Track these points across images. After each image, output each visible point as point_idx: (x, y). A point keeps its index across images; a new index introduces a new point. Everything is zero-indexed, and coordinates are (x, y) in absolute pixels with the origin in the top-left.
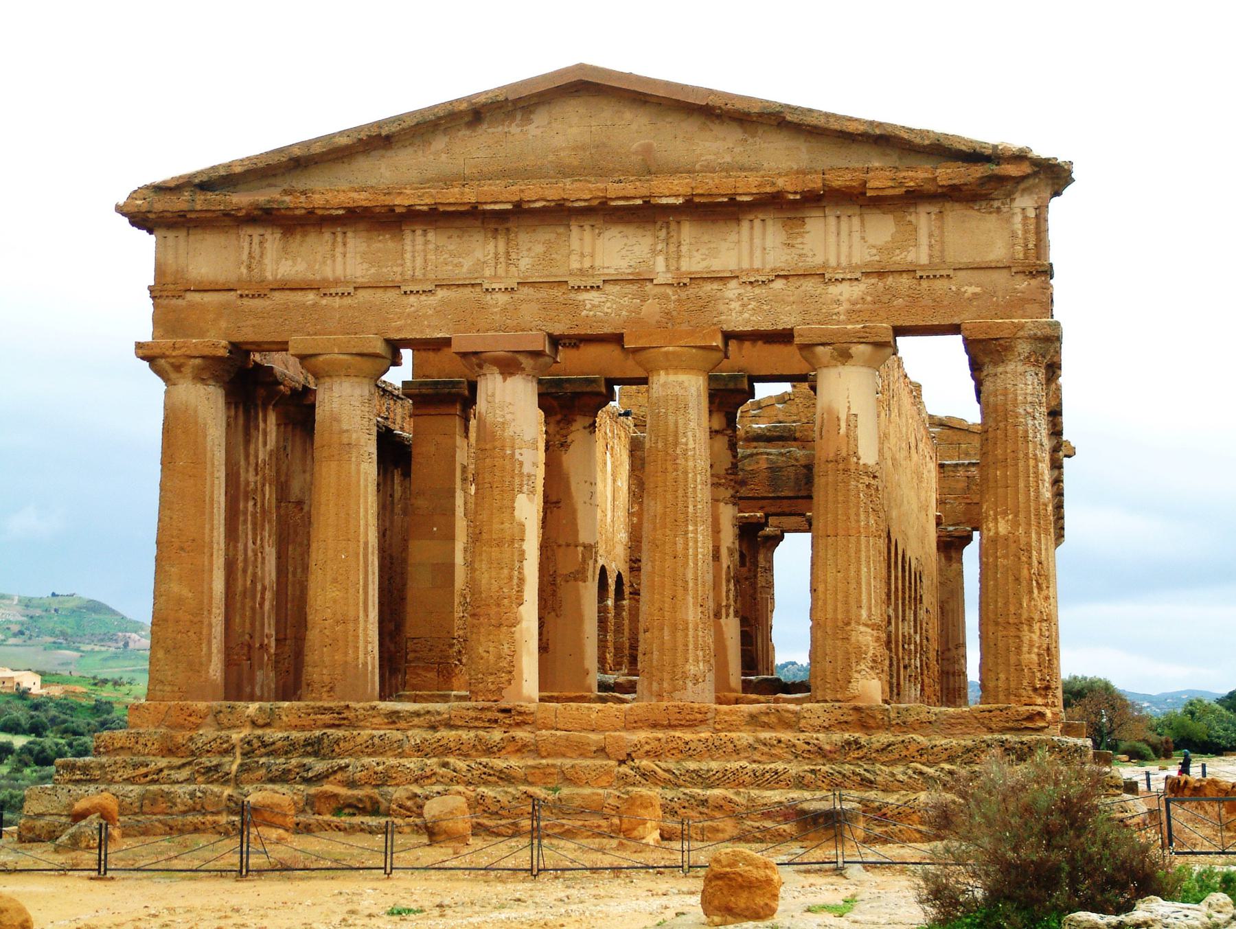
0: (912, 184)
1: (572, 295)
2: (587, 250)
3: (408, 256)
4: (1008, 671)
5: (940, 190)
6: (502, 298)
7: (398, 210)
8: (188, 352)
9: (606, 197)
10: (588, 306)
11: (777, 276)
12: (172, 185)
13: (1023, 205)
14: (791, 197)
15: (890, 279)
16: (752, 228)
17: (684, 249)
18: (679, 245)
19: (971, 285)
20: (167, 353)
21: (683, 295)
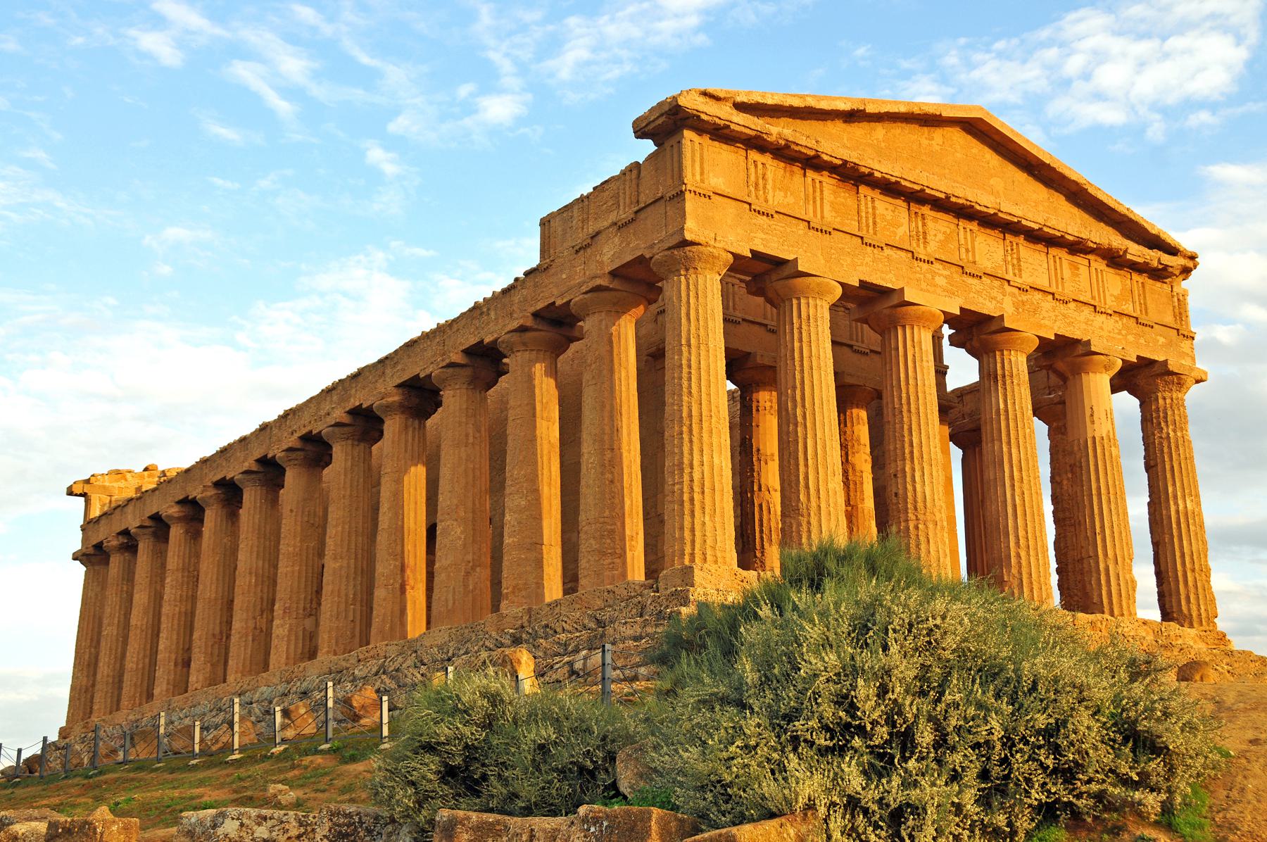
0: (1148, 257)
1: (965, 278)
2: (970, 247)
3: (863, 214)
4: (1206, 604)
5: (1160, 267)
6: (925, 266)
7: (877, 174)
8: (726, 247)
9: (999, 211)
10: (974, 290)
11: (1073, 300)
12: (722, 95)
13: (1178, 291)
14: (1092, 245)
15: (1125, 319)
16: (1055, 262)
17: (1022, 264)
18: (1019, 260)
19: (1161, 335)
20: (712, 243)
21: (1025, 297)
